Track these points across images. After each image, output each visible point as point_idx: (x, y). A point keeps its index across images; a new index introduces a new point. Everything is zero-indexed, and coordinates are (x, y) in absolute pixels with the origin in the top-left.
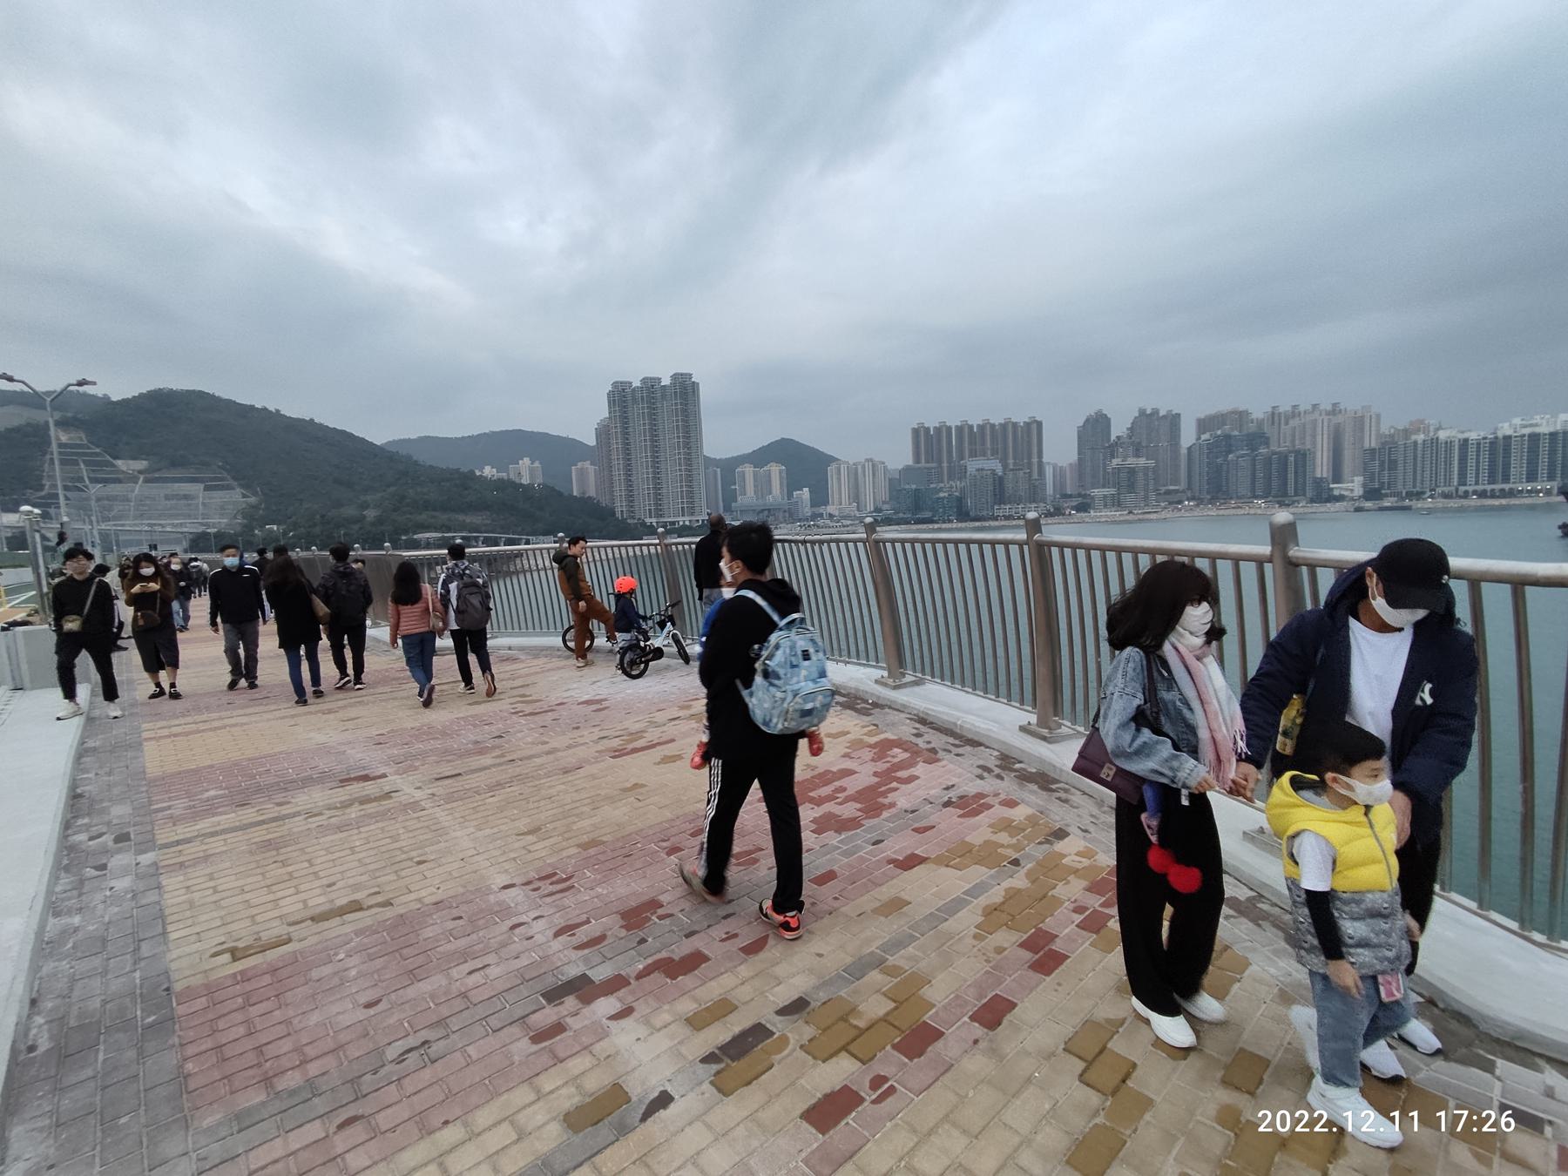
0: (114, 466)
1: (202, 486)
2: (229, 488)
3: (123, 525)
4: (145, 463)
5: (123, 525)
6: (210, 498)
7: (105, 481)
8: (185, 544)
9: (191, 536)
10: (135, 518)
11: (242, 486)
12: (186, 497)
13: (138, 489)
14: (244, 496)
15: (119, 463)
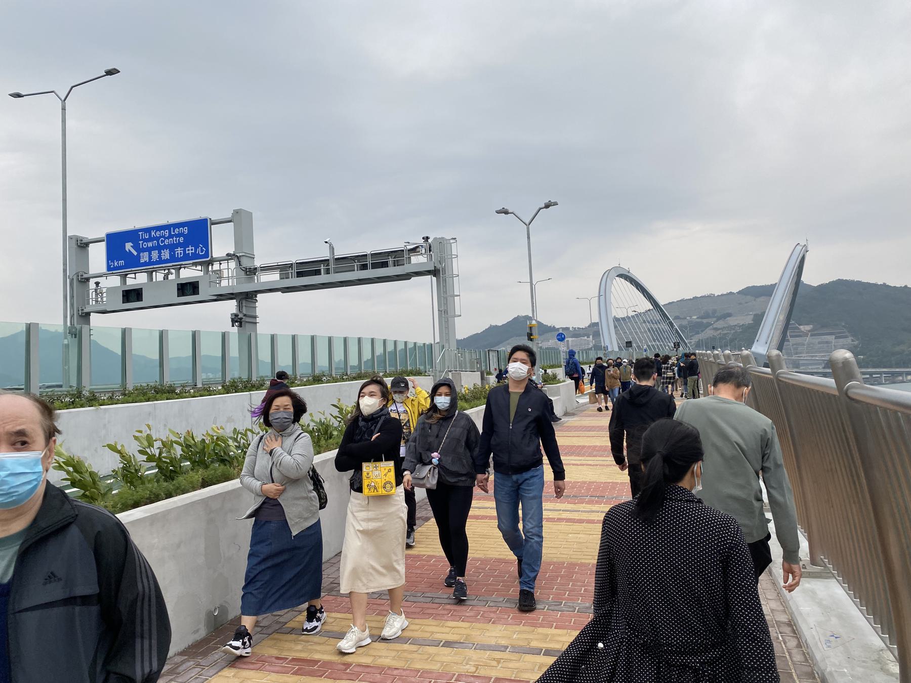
0: (799, 329)
1: (834, 337)
2: (846, 337)
3: (801, 357)
4: (811, 326)
5: (801, 357)
6: (837, 342)
7: (797, 336)
8: (823, 365)
9: (826, 362)
10: (807, 353)
11: (852, 336)
12: (827, 342)
13: (808, 339)
14: (853, 341)
15: (801, 327)
